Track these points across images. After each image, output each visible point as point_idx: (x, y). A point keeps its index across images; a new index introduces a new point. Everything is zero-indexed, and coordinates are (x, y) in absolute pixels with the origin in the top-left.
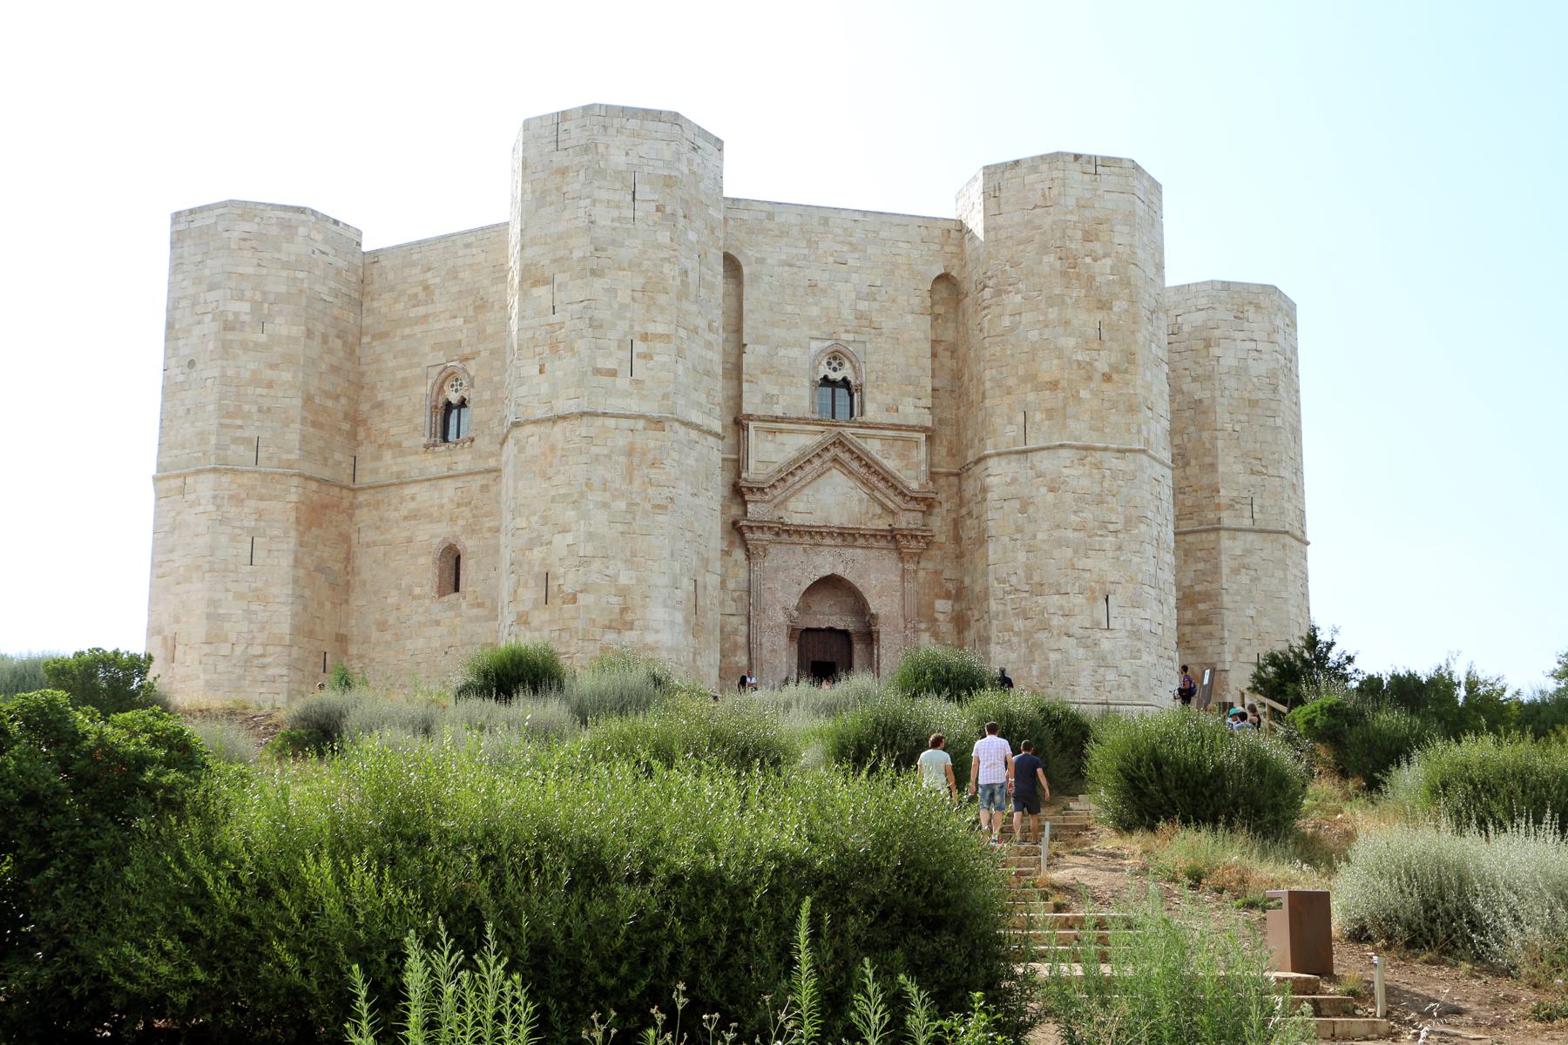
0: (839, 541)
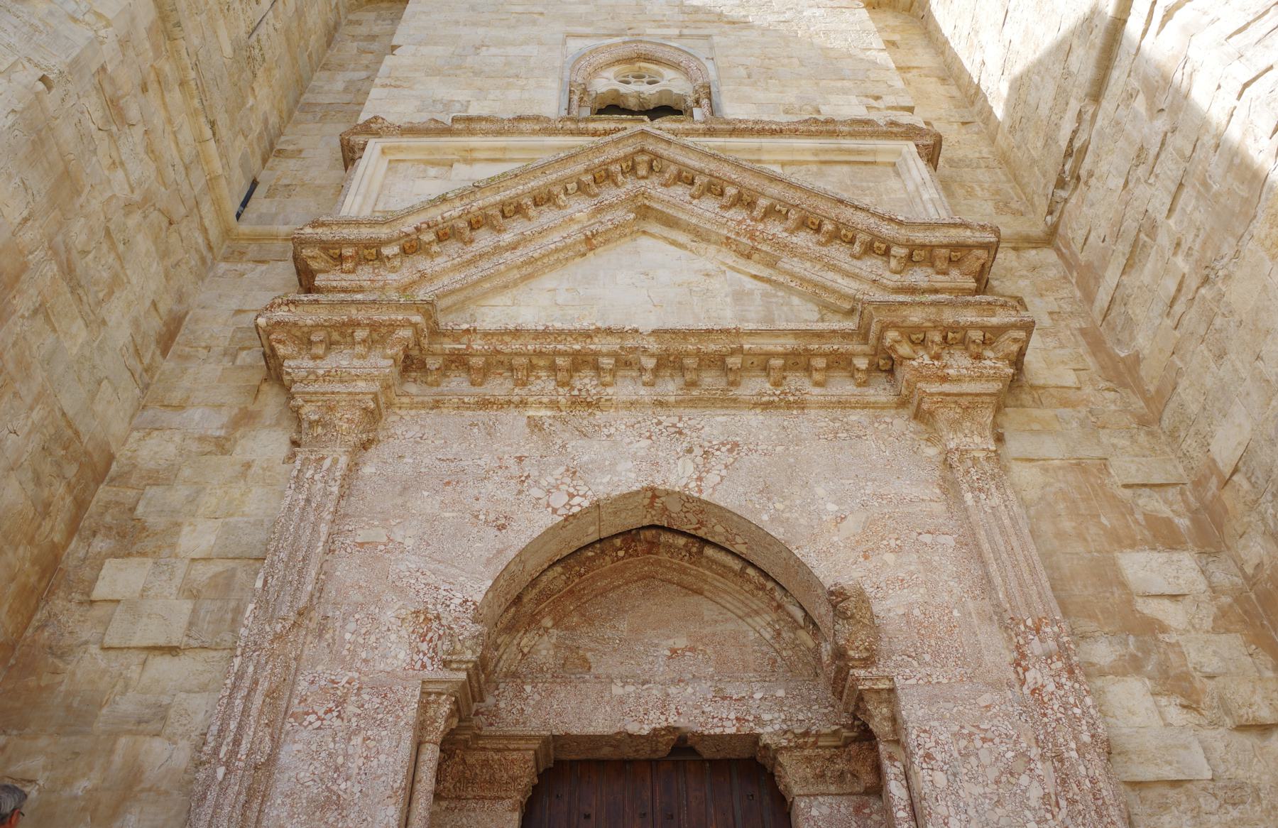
0: (670, 387)
